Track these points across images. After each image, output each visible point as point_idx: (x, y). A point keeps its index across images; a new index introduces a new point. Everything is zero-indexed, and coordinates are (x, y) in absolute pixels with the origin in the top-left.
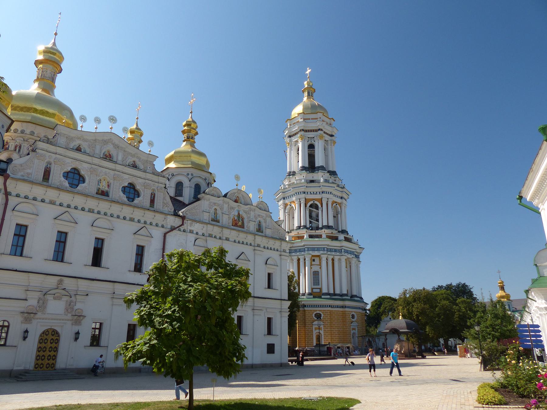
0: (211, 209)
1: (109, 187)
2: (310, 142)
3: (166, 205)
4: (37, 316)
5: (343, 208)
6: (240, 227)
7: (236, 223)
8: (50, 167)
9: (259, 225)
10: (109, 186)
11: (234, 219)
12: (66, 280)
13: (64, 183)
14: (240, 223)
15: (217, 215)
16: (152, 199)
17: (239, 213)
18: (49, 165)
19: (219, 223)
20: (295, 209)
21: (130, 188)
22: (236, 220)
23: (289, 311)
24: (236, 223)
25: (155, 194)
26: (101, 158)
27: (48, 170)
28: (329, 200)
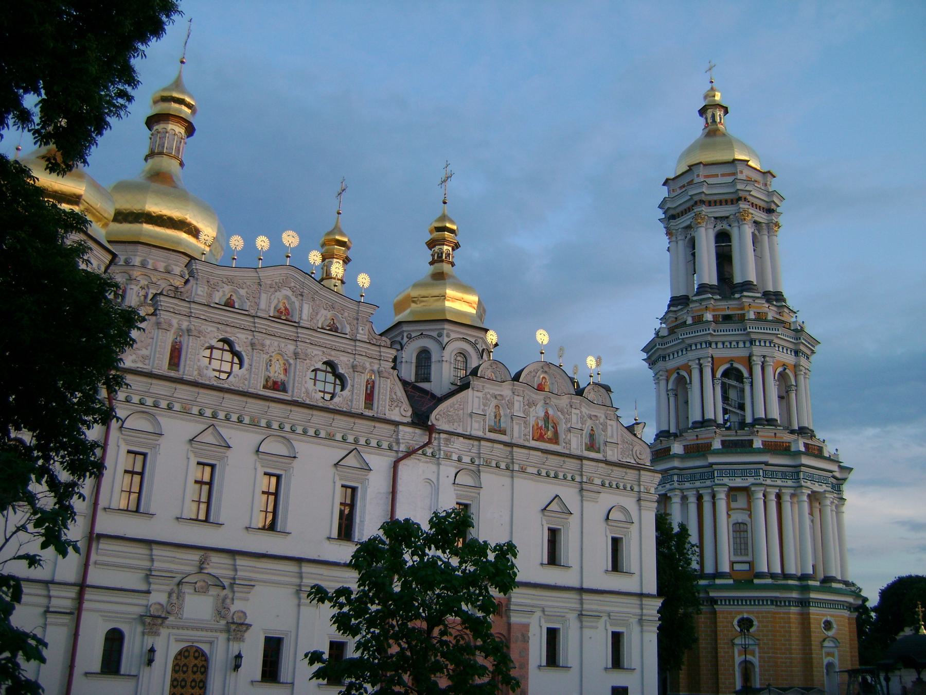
0: (486, 408)
1: (286, 372)
2: (719, 227)
3: (396, 404)
5: (801, 378)
6: (550, 441)
7: (541, 434)
8: (180, 342)
9: (592, 436)
11: (537, 425)
12: (215, 558)
14: (550, 434)
16: (369, 392)
17: (547, 413)
18: (178, 338)
19: (505, 435)
20: (688, 382)
21: (326, 372)
22: (541, 427)
23: (659, 619)
24: (541, 434)
25: (373, 382)
26: (270, 318)
27: (177, 347)
28: (767, 359)
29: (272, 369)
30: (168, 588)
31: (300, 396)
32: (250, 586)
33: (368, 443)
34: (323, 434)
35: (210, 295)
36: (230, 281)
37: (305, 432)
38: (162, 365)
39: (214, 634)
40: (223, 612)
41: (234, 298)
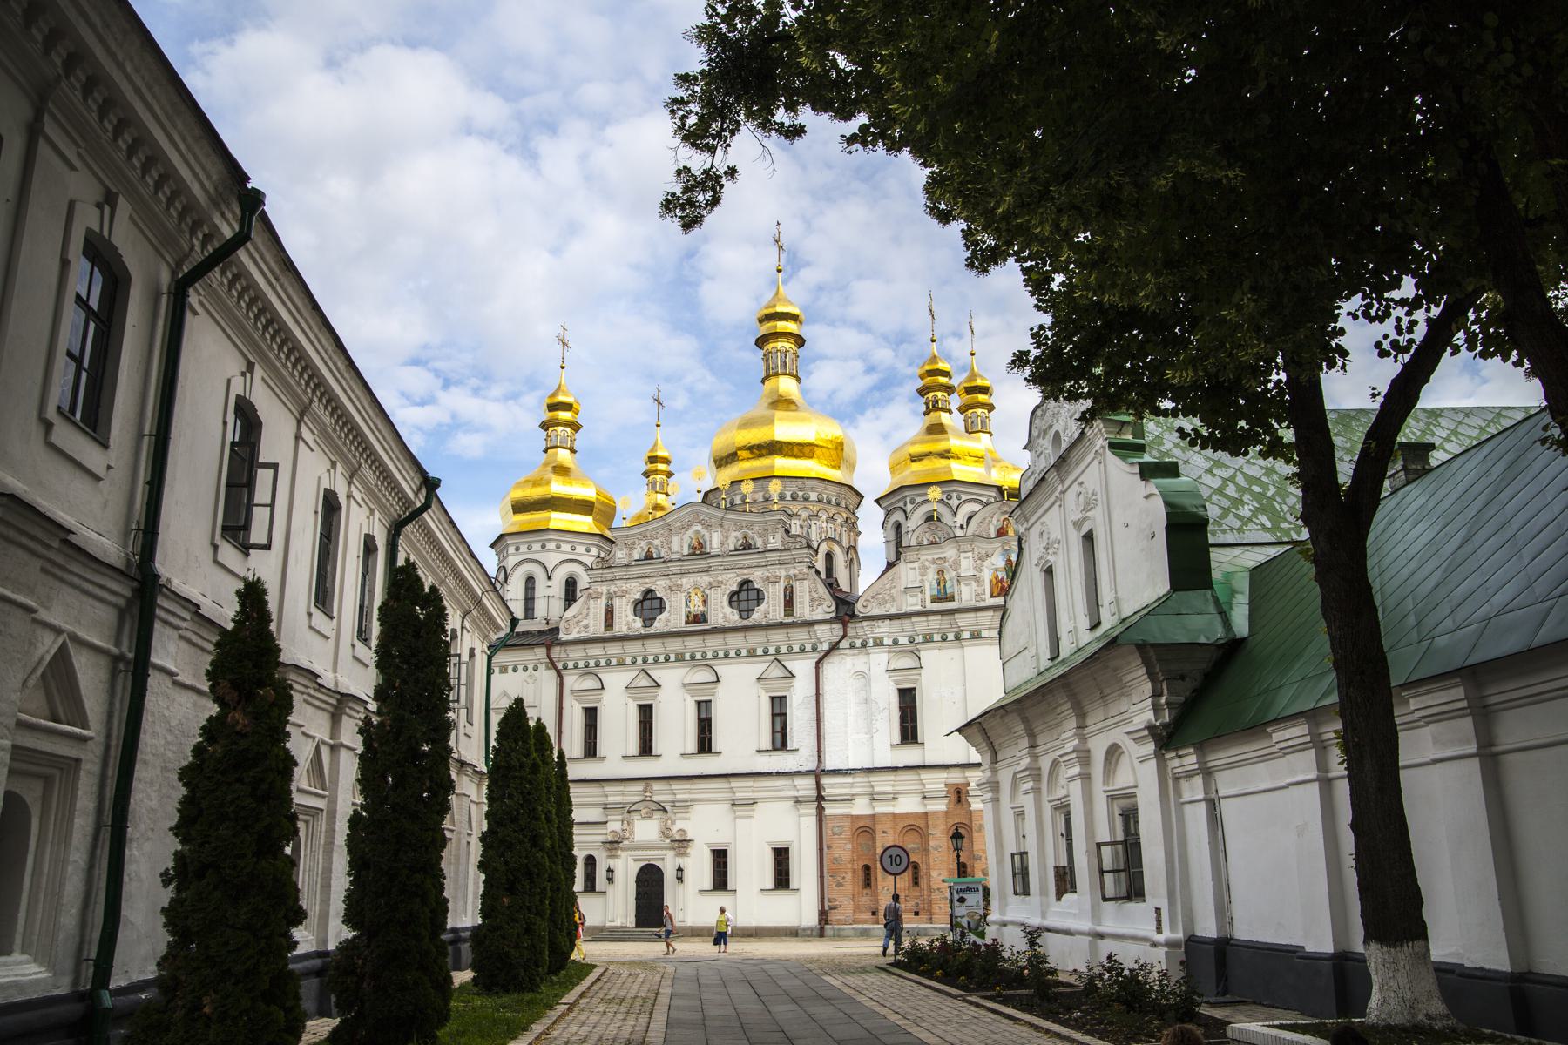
4: (621, 845)
10: (704, 602)
11: (996, 578)
12: (657, 786)
13: (633, 624)
15: (945, 586)
22: (1002, 579)
30: (620, 818)
31: (721, 622)
32: (686, 806)
33: (790, 650)
34: (744, 653)
35: (631, 556)
36: (644, 536)
37: (726, 655)
38: (598, 629)
39: (664, 852)
40: (666, 832)
41: (653, 550)
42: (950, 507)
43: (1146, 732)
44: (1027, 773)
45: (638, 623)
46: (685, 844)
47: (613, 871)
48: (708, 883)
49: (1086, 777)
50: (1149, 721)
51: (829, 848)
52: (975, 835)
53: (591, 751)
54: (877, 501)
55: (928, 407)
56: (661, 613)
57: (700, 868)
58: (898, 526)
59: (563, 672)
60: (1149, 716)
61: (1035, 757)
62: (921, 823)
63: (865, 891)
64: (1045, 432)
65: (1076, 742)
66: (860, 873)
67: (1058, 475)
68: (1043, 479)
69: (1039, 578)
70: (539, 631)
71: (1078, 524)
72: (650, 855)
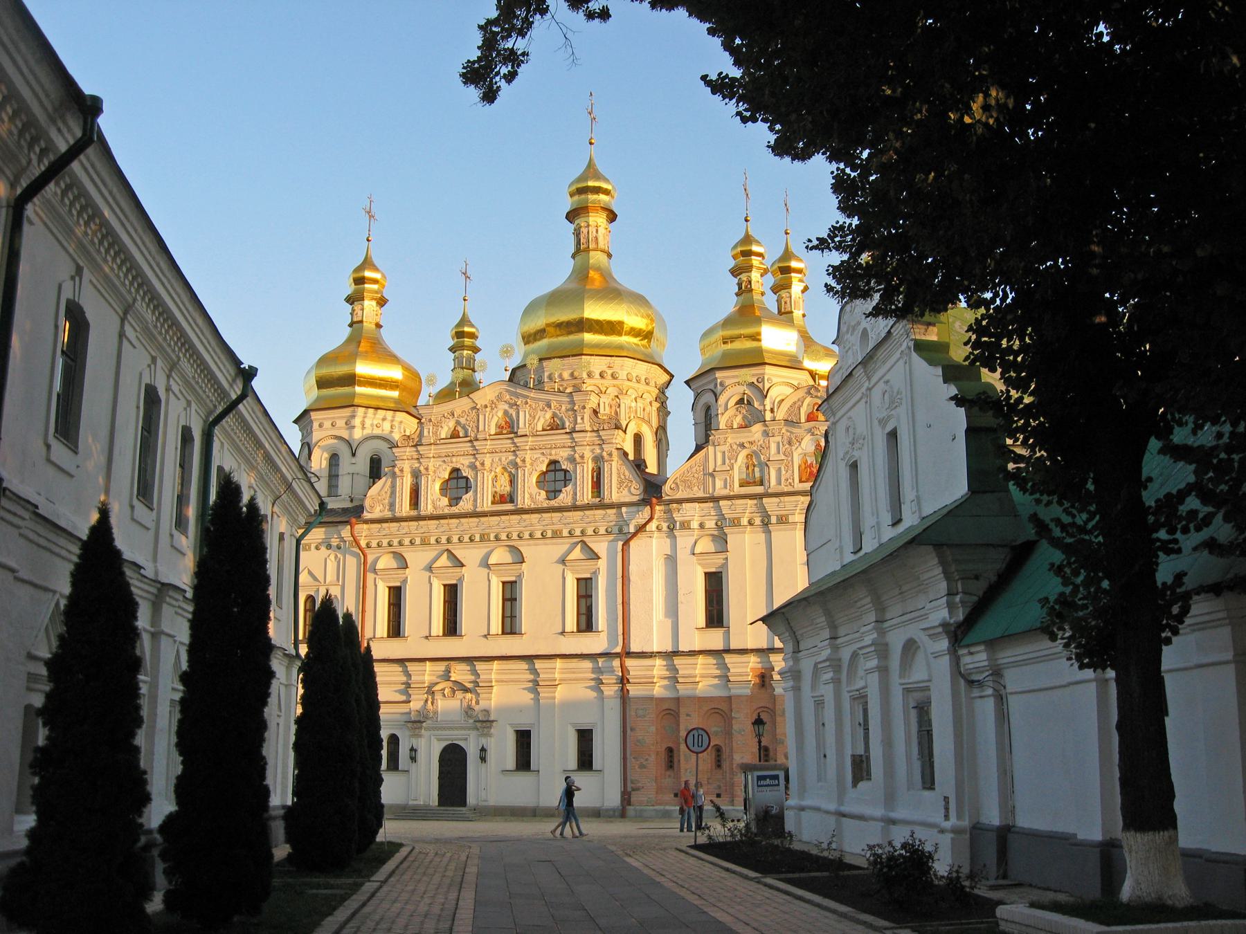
4: (424, 724)
10: (511, 482)
16: (595, 479)
22: (812, 464)
29: (498, 485)
34: (549, 534)
35: (435, 433)
38: (404, 508)
41: (459, 428)
42: (761, 391)
43: (940, 630)
44: (828, 663)
45: (445, 501)
46: (488, 724)
47: (416, 751)
48: (511, 762)
49: (883, 670)
50: (944, 618)
51: (632, 730)
52: (778, 719)
53: (395, 630)
54: (687, 382)
55: (740, 288)
56: (467, 493)
57: (504, 749)
58: (708, 409)
59: (367, 551)
60: (944, 613)
61: (836, 648)
62: (724, 707)
63: (668, 773)
64: (854, 330)
65: (875, 635)
66: (663, 755)
67: (865, 372)
68: (851, 374)
69: (844, 473)
70: (343, 509)
71: (883, 422)
72: (456, 737)
